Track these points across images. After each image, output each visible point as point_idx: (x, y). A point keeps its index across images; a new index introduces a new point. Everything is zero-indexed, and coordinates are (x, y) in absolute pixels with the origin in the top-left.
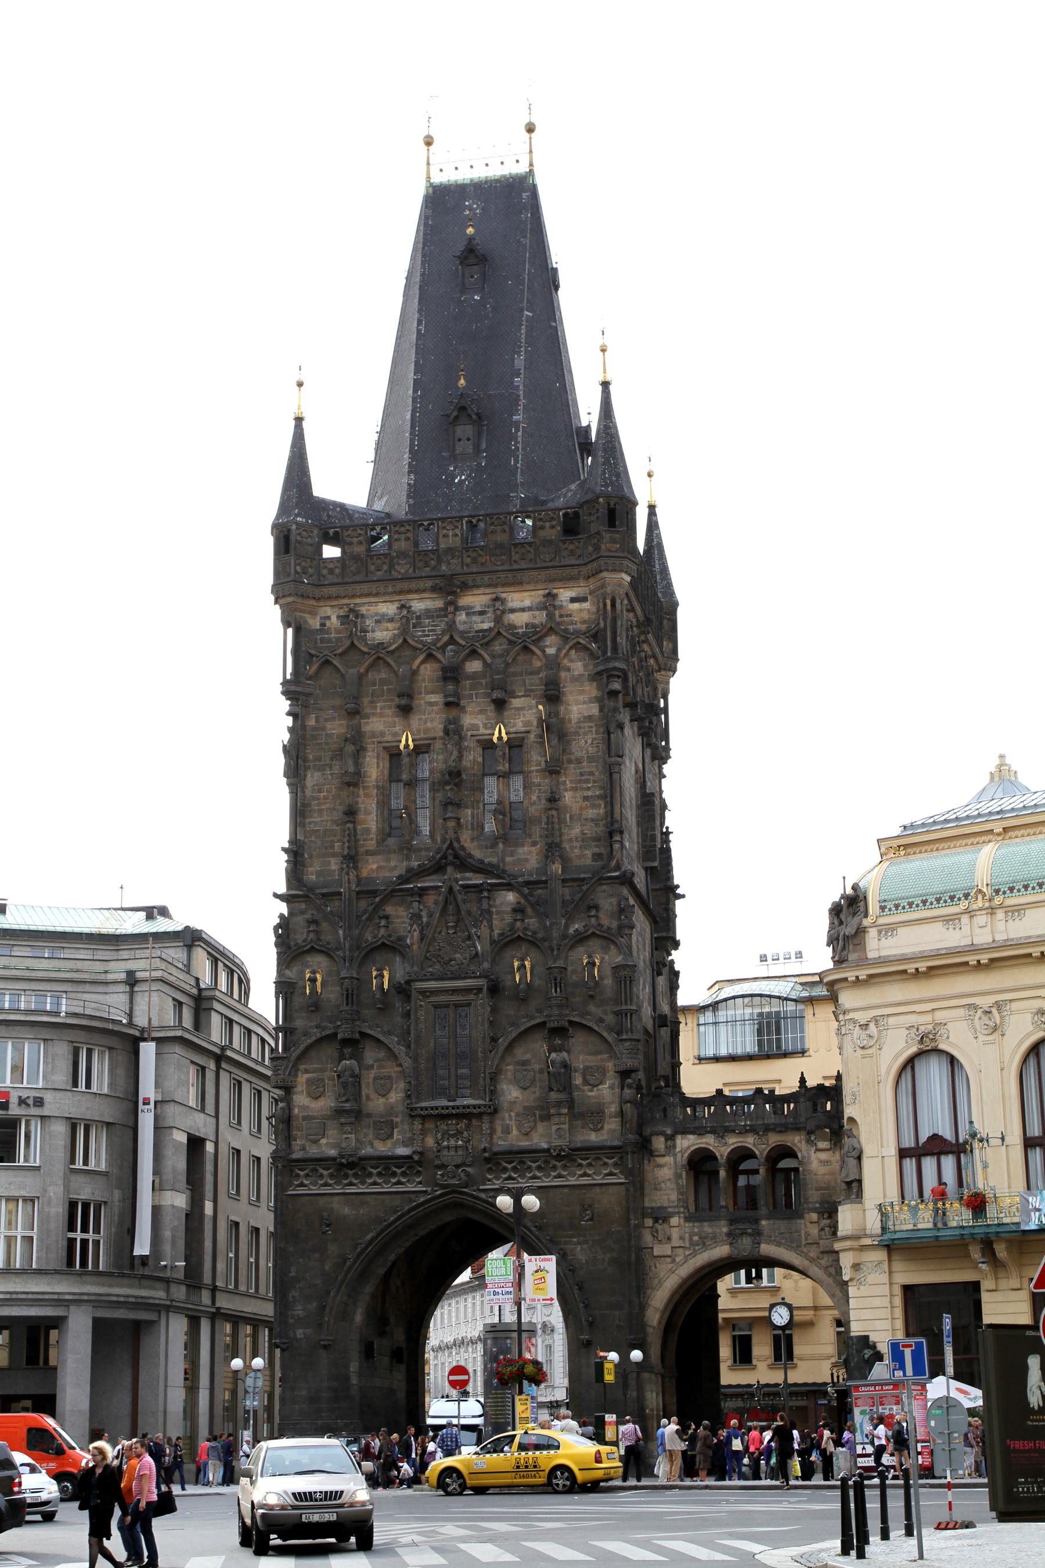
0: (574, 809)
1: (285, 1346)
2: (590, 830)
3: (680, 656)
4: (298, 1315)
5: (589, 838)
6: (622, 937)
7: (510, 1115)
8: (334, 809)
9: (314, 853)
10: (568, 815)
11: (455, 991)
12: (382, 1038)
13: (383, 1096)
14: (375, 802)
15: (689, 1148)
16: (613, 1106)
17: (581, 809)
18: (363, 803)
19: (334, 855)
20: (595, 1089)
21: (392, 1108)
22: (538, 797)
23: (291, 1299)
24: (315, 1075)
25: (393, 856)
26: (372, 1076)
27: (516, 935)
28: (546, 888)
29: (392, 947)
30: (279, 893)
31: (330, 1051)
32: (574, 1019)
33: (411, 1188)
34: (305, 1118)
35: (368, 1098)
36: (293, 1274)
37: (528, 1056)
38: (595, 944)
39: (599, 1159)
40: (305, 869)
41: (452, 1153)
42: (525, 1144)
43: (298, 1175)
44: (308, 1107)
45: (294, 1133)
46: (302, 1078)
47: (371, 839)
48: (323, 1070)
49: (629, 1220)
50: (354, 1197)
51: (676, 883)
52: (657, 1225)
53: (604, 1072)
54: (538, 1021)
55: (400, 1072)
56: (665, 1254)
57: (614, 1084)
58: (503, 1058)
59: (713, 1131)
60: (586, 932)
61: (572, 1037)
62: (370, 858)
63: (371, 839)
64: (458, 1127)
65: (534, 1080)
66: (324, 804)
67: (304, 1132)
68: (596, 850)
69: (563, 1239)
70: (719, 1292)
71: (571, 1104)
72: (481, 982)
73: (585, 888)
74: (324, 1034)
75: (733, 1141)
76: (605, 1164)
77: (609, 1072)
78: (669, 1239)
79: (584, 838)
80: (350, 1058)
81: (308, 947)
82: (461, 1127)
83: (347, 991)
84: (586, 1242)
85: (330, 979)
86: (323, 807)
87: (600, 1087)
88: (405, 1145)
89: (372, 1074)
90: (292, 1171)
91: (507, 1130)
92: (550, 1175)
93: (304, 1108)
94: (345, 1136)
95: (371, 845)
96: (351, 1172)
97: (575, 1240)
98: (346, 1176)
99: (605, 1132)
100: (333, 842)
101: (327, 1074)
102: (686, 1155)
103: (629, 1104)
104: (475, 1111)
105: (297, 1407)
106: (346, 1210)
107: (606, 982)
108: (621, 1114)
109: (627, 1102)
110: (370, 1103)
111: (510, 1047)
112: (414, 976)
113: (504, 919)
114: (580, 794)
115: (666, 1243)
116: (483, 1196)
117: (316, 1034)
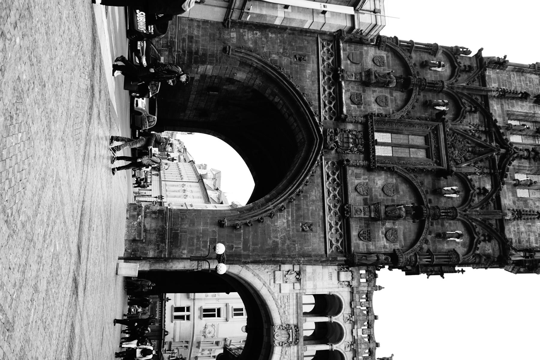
0: (534, 228)
1: (226, 24)
2: (524, 235)
3: (518, 274)
4: (245, 35)
5: (520, 237)
6: (473, 257)
7: (366, 179)
8: (522, 88)
9: (499, 75)
10: (530, 224)
11: (438, 149)
12: (410, 102)
13: (376, 101)
14: (527, 112)
16: (374, 248)
17: (534, 232)
18: (526, 105)
19: (499, 85)
20: (384, 236)
21: (369, 105)
22: (538, 206)
23: (255, 32)
24: (386, 61)
25: (502, 119)
27: (471, 189)
28: (495, 209)
31: (399, 71)
32: (426, 224)
33: (323, 112)
34: (361, 53)
35: (374, 91)
36: (270, 35)
37: (401, 193)
38: (466, 239)
39: (341, 237)
40: (491, 69)
41: (345, 140)
42: (350, 188)
43: (328, 45)
46: (383, 54)
47: (509, 108)
49: (304, 257)
50: (317, 77)
51: (445, 275)
52: (295, 274)
53: (393, 242)
54: (425, 200)
55: (389, 112)
56: (276, 279)
57: (387, 248)
58: (400, 176)
59: (353, 313)
60: (476, 233)
61: (414, 222)
62: (499, 106)
63: (509, 108)
64: (360, 145)
65: (388, 196)
66: (524, 83)
67: (353, 51)
68: (514, 241)
70: (231, 293)
71: (375, 220)
72: (445, 166)
73: (499, 234)
75: (346, 327)
76: (337, 241)
77: (394, 245)
78: (286, 282)
79: (519, 233)
81: (456, 65)
84: (288, 226)
85: (438, 76)
87: (385, 239)
88: (347, 111)
89: (388, 96)
90: (331, 41)
91: (357, 176)
92: (330, 203)
93: (367, 53)
94: (354, 75)
95: (506, 107)
96: (331, 76)
97: (290, 219)
98: (329, 73)
99: (358, 241)
100: (506, 86)
101: (386, 68)
102: (338, 295)
103: (376, 258)
105: (187, 28)
106: (308, 72)
107: (445, 245)
108: (370, 253)
109: (378, 257)
110: (371, 92)
111: (406, 181)
113: (476, 182)
115: (283, 280)
116: (318, 158)
117: (411, 63)
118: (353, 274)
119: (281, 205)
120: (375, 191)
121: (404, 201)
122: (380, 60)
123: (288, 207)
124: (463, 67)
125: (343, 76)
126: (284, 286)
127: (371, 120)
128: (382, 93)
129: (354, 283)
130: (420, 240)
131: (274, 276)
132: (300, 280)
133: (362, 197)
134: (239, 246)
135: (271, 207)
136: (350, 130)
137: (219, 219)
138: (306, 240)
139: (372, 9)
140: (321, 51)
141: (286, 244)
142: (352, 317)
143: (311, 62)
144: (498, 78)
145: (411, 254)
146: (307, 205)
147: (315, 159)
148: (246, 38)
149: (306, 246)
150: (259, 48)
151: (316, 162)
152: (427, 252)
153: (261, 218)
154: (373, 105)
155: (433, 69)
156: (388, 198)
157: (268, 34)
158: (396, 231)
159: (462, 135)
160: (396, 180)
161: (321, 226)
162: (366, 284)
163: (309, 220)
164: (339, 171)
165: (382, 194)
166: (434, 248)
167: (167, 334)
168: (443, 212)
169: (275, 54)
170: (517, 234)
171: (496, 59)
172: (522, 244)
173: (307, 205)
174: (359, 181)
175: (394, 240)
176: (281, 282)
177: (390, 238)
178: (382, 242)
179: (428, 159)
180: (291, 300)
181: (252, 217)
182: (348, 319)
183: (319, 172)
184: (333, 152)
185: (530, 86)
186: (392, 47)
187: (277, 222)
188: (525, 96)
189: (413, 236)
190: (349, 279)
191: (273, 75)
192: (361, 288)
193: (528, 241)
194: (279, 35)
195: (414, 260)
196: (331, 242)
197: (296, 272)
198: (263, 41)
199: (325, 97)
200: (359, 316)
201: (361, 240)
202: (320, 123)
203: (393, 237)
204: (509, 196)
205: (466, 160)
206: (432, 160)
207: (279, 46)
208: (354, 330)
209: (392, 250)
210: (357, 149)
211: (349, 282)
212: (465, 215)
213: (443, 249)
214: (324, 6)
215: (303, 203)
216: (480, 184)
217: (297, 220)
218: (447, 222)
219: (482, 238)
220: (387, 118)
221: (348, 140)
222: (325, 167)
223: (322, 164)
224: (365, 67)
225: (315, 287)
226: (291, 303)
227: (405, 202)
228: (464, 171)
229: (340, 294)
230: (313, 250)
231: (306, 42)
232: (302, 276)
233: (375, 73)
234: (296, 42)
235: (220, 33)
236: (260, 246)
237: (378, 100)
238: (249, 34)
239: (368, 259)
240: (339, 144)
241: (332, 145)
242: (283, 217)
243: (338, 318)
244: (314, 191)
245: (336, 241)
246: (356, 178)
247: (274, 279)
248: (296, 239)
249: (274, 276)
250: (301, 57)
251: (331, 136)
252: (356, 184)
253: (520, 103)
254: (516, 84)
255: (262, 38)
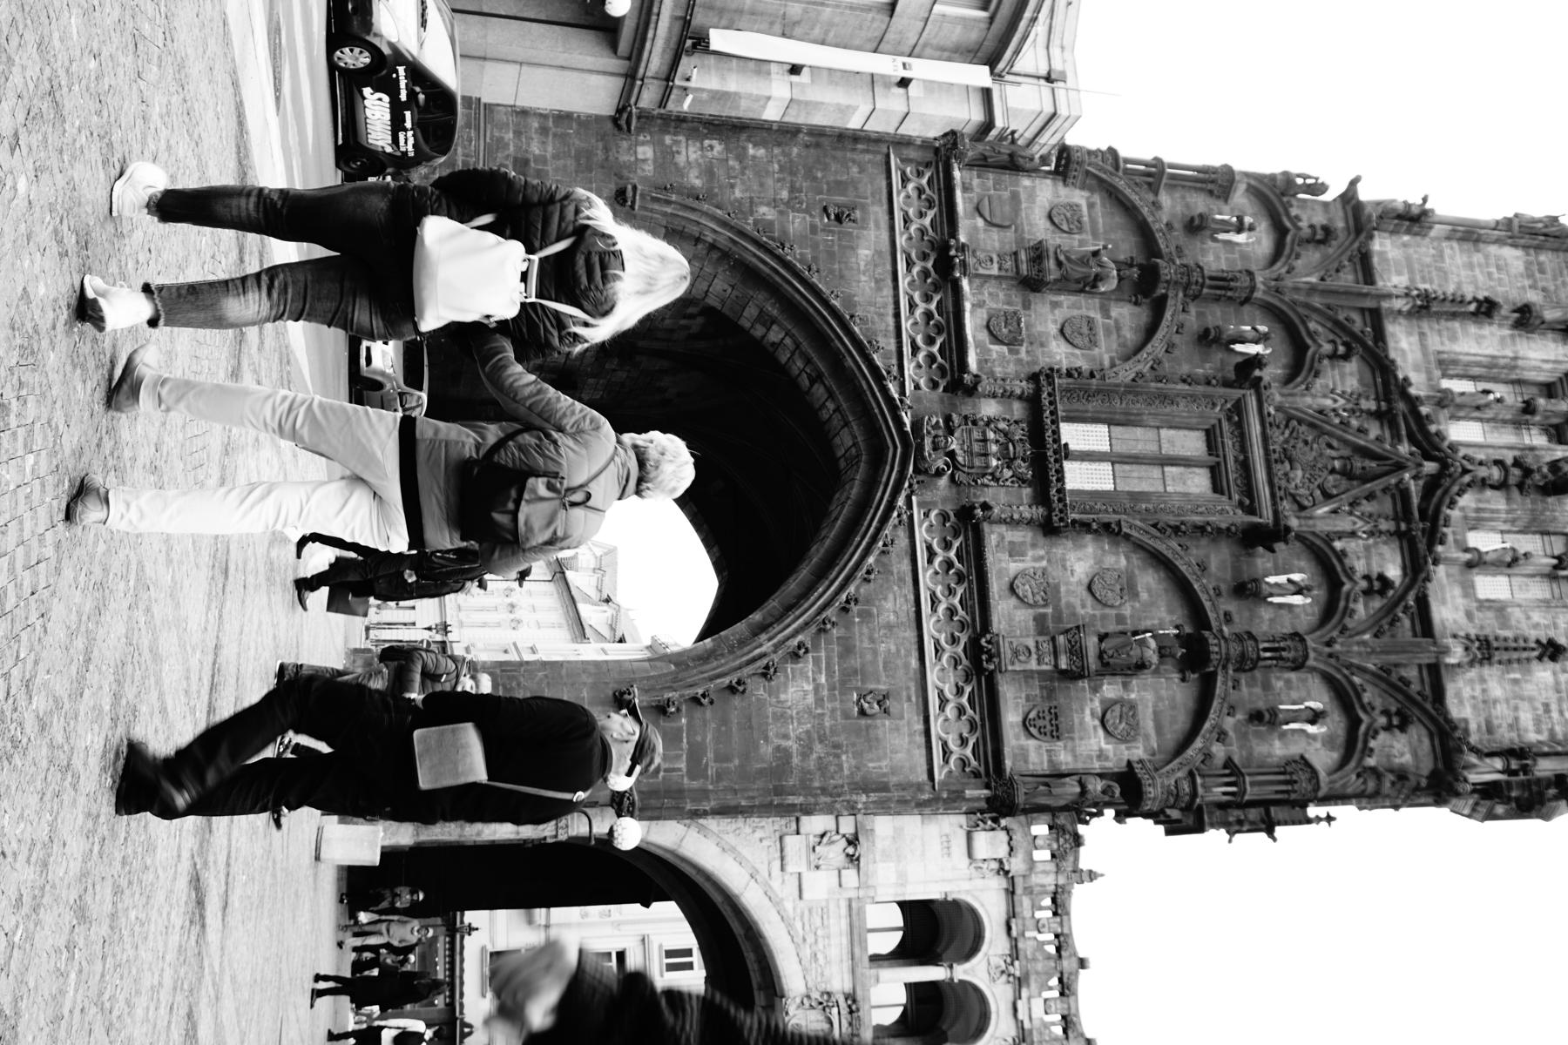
1: (623, 122)
2: (1501, 713)
3: (1489, 823)
4: (678, 152)
5: (1490, 716)
6: (1359, 776)
7: (1041, 558)
8: (1477, 288)
10: (1518, 676)
11: (1245, 467)
12: (1160, 334)
13: (1062, 331)
14: (1496, 353)
15: (983, 905)
16: (1070, 759)
17: (1531, 700)
18: (1492, 334)
19: (1412, 280)
20: (1097, 723)
21: (1042, 345)
23: (707, 142)
26: (1092, 314)
27: (1344, 579)
28: (1415, 635)
29: (1300, 365)
30: (1360, 186)
31: (1125, 245)
32: (1219, 684)
33: (909, 368)
34: (1015, 197)
35: (1055, 305)
36: (751, 151)
37: (1144, 596)
38: (1334, 724)
40: (1386, 235)
41: (976, 447)
42: (996, 587)
43: (920, 174)
44: (1034, 202)
45: (991, 176)
46: (1079, 197)
47: (1442, 343)
48: (1095, 234)
49: (866, 791)
50: (889, 267)
52: (843, 843)
53: (1126, 739)
54: (1212, 616)
55: (1101, 364)
56: (788, 859)
57: (1107, 758)
58: (1139, 547)
59: (1015, 954)
60: (1363, 707)
61: (1183, 680)
62: (1415, 339)
63: (1442, 343)
64: (1019, 461)
65: (1105, 605)
66: (1482, 272)
67: (992, 192)
68: (1473, 726)
69: (823, 654)
70: (655, 905)
73: (1428, 706)
74: (1158, 235)
75: (998, 995)
76: (963, 742)
77: (1128, 749)
78: (817, 867)
79: (1488, 702)
80: (1120, 279)
81: (1288, 224)
82: (1020, 467)
83: (1232, 280)
84: (819, 701)
85: (1237, 256)
86: (1477, 271)
87: (1101, 732)
88: (980, 363)
89: (1097, 316)
90: (928, 165)
91: (1015, 551)
92: (939, 631)
93: (1032, 197)
94: (995, 259)
95: (1435, 342)
96: (929, 265)
97: (823, 679)
98: (924, 257)
100: (1431, 282)
101: (1088, 237)
103: (1078, 790)
104: (1053, 491)
105: (511, 135)
106: (864, 253)
107: (1277, 743)
112: (1265, 393)
113: (1358, 558)
114: (1552, 698)
115: (809, 863)
116: (901, 502)
117: (1158, 222)
118: (1011, 839)
119: (795, 642)
120: (1068, 591)
121: (1153, 618)
122: (1068, 215)
123: (816, 647)
124: (1306, 232)
125: (964, 264)
126: (810, 877)
127: (1050, 389)
128: (1080, 308)
129: (1016, 865)
130: (1203, 732)
131: (782, 850)
132: (858, 859)
133: (1031, 611)
134: (677, 766)
135: (767, 647)
136: (989, 418)
137: (616, 686)
138: (872, 742)
139: (1043, 72)
140: (899, 193)
141: (814, 756)
142: (1012, 964)
143: (872, 225)
144: (1408, 259)
145: (1180, 774)
146: (872, 640)
147: (891, 506)
148: (681, 160)
149: (871, 760)
150: (720, 187)
151: (895, 514)
152: (1225, 767)
153: (739, 682)
154: (1054, 343)
155: (1222, 236)
156: (1107, 611)
157: (745, 149)
158: (1132, 706)
159: (1312, 425)
160: (1127, 558)
161: (914, 699)
162: (1051, 867)
163: (878, 682)
164: (961, 538)
165: (1089, 600)
166: (1244, 753)
167: (470, 1034)
168: (1266, 650)
169: (768, 205)
170: (1481, 706)
171: (1401, 207)
172: (1497, 736)
173: (872, 640)
174: (1021, 566)
175: (1128, 734)
176: (803, 869)
177: (1116, 728)
178: (1093, 741)
179: (1217, 496)
180: (832, 921)
181: (711, 679)
182: (1003, 972)
183: (902, 541)
184: (943, 481)
185: (1500, 279)
186: (1104, 176)
187: (785, 692)
188: (1486, 309)
189: (1181, 722)
190: (1002, 851)
191: (762, 266)
192: (1036, 879)
193: (1515, 725)
194: (776, 151)
195: (1187, 790)
196: (945, 745)
197: (844, 836)
198: (733, 168)
199: (916, 323)
200: (1034, 959)
201: (1032, 736)
202: (901, 401)
203: (1123, 725)
204: (1453, 597)
205: (1328, 496)
206: (1230, 498)
207: (779, 180)
208: (1020, 1004)
209: (1124, 764)
210: (1010, 473)
211: (1001, 862)
212: (1330, 655)
213: (1270, 755)
214: (904, 65)
215: (861, 634)
216: (1368, 564)
217: (843, 683)
218: (1278, 678)
219: (1383, 720)
220: (1094, 381)
221: (985, 447)
222: (920, 526)
223: (911, 517)
224: (1027, 236)
225: (902, 879)
226: (834, 929)
227: (1156, 622)
228: (1323, 527)
229: (976, 898)
230: (894, 771)
231: (855, 169)
232: (863, 848)
233: (1056, 253)
234: (825, 168)
235: (606, 149)
236: (737, 762)
237: (1068, 331)
238: (691, 149)
239: (1055, 791)
240: (960, 459)
241: (940, 464)
242: (803, 675)
243: (973, 969)
244: (891, 596)
245: (959, 742)
246: (1010, 556)
247: (782, 859)
248: (842, 739)
249: (782, 850)
250: (843, 213)
251: (936, 436)
252: (1012, 573)
253: (1473, 329)
254: (1458, 275)
255: (727, 160)
